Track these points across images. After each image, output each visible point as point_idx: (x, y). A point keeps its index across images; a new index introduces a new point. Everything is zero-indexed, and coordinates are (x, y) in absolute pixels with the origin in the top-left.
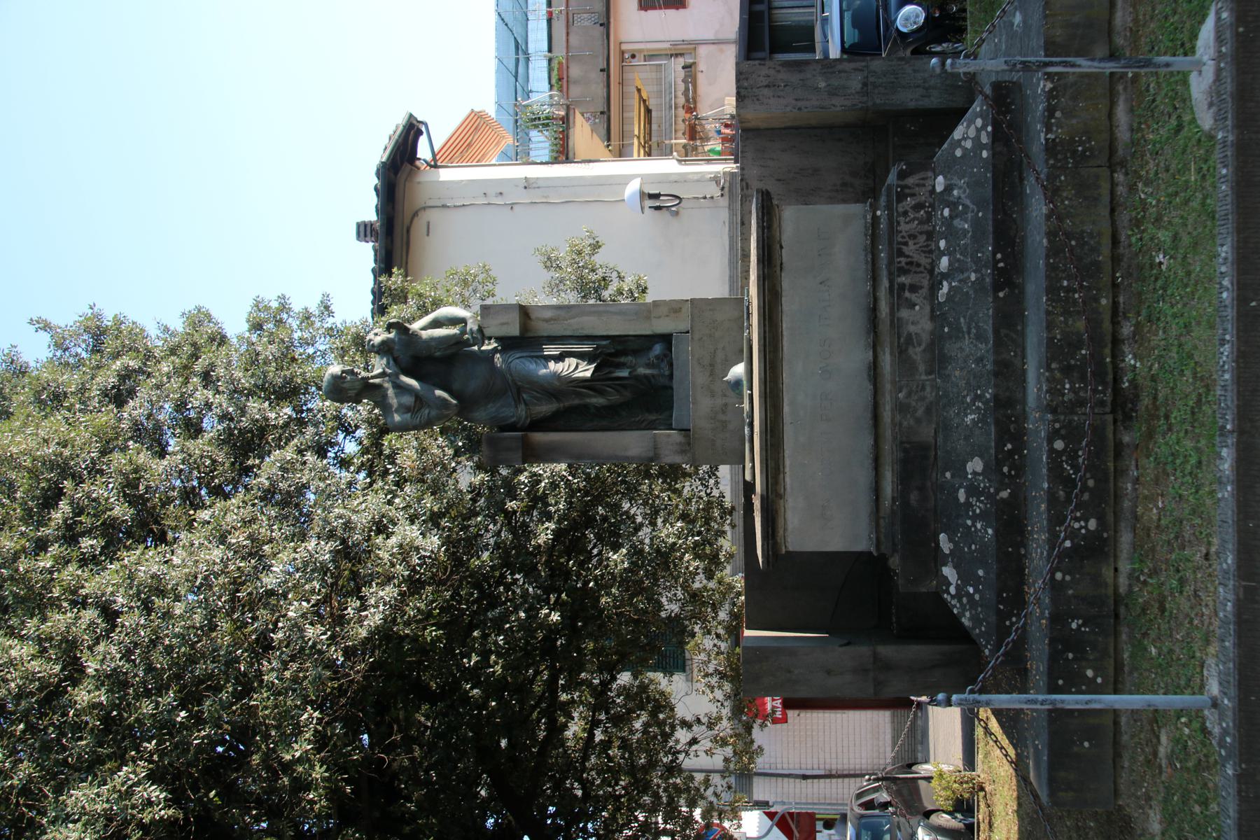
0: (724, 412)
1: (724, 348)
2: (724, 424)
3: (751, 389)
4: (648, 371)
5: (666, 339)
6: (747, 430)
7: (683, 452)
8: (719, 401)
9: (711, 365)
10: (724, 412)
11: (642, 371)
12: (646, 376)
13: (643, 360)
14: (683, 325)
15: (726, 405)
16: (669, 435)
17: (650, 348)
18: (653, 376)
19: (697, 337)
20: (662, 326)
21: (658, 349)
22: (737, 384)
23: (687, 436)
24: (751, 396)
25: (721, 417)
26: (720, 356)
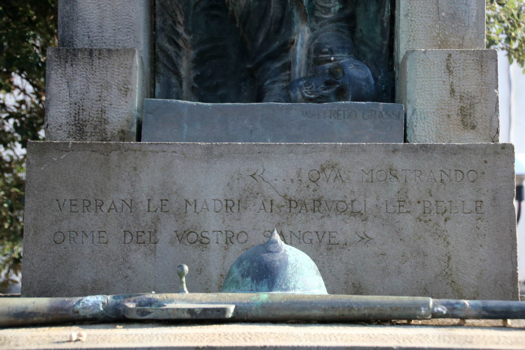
0: (182, 236)
1: (365, 239)
2: (146, 237)
3: (237, 319)
4: (300, 52)
5: (387, 88)
6: (96, 301)
7: (79, 128)
8: (213, 224)
9: (318, 201)
10: (182, 236)
11: (302, 36)
12: (287, 46)
13: (329, 36)
14: (425, 130)
15: (202, 242)
16: (126, 91)
17: (358, 56)
18: (288, 66)
19: (400, 162)
20: (424, 85)
21: (358, 72)
22: (264, 272)
23: (123, 135)
24: (215, 318)
25: (168, 230)
26: (345, 228)
